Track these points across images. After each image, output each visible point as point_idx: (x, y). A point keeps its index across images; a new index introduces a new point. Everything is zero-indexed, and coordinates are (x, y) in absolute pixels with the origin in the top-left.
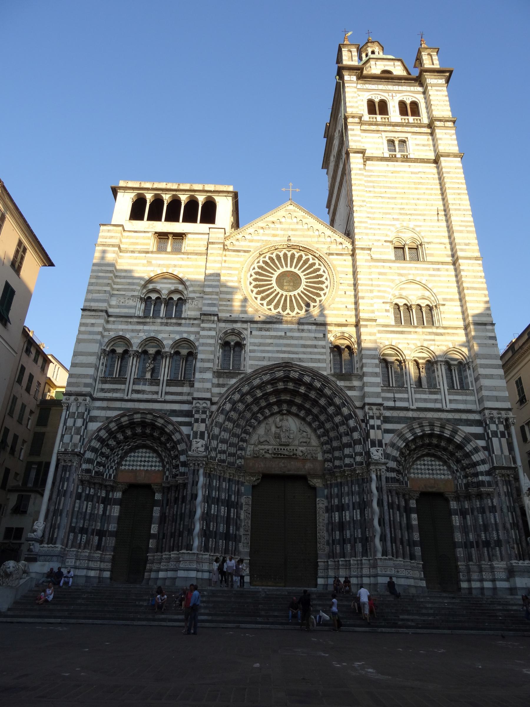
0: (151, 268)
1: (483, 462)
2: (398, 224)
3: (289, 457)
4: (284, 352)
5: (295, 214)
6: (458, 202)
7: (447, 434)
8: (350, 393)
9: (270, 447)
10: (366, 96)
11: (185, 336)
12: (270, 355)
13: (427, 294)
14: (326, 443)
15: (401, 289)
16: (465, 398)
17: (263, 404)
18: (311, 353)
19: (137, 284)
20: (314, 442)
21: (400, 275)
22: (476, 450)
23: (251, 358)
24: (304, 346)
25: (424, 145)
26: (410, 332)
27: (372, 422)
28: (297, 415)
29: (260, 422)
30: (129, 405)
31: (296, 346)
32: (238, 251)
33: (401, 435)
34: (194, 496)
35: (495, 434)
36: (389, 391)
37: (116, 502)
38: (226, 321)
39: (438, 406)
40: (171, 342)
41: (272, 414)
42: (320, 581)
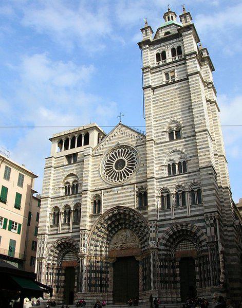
0: (65, 173)
1: (205, 240)
2: (169, 120)
3: (127, 249)
4: (119, 201)
5: (121, 129)
6: (197, 100)
7: (189, 228)
8: (145, 216)
9: (119, 245)
10: (155, 52)
11: (78, 201)
12: (111, 204)
13: (183, 155)
14: (141, 240)
15: (171, 156)
16: (199, 208)
17: (113, 226)
18: (128, 199)
19: (61, 182)
20: (137, 240)
21: (169, 148)
22: (202, 234)
23: (104, 207)
24: (126, 196)
25: (183, 71)
26: (173, 179)
27: (151, 229)
28: (129, 228)
29: (114, 235)
30: (60, 236)
31: (122, 197)
32: (98, 155)
33: (167, 233)
34: (82, 271)
35: (208, 225)
36: (162, 212)
37: (62, 274)
38: (93, 191)
39: (185, 215)
40: (73, 205)
41: (119, 230)
42: (140, 301)
